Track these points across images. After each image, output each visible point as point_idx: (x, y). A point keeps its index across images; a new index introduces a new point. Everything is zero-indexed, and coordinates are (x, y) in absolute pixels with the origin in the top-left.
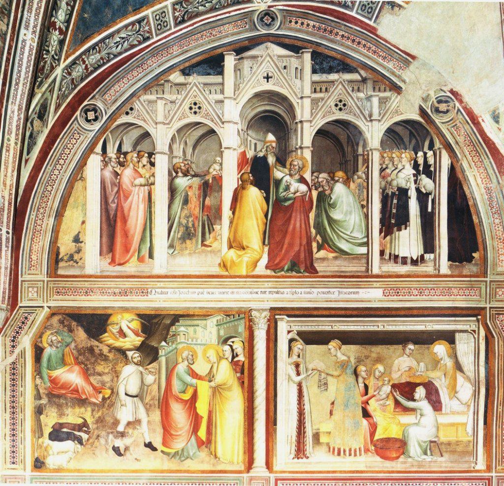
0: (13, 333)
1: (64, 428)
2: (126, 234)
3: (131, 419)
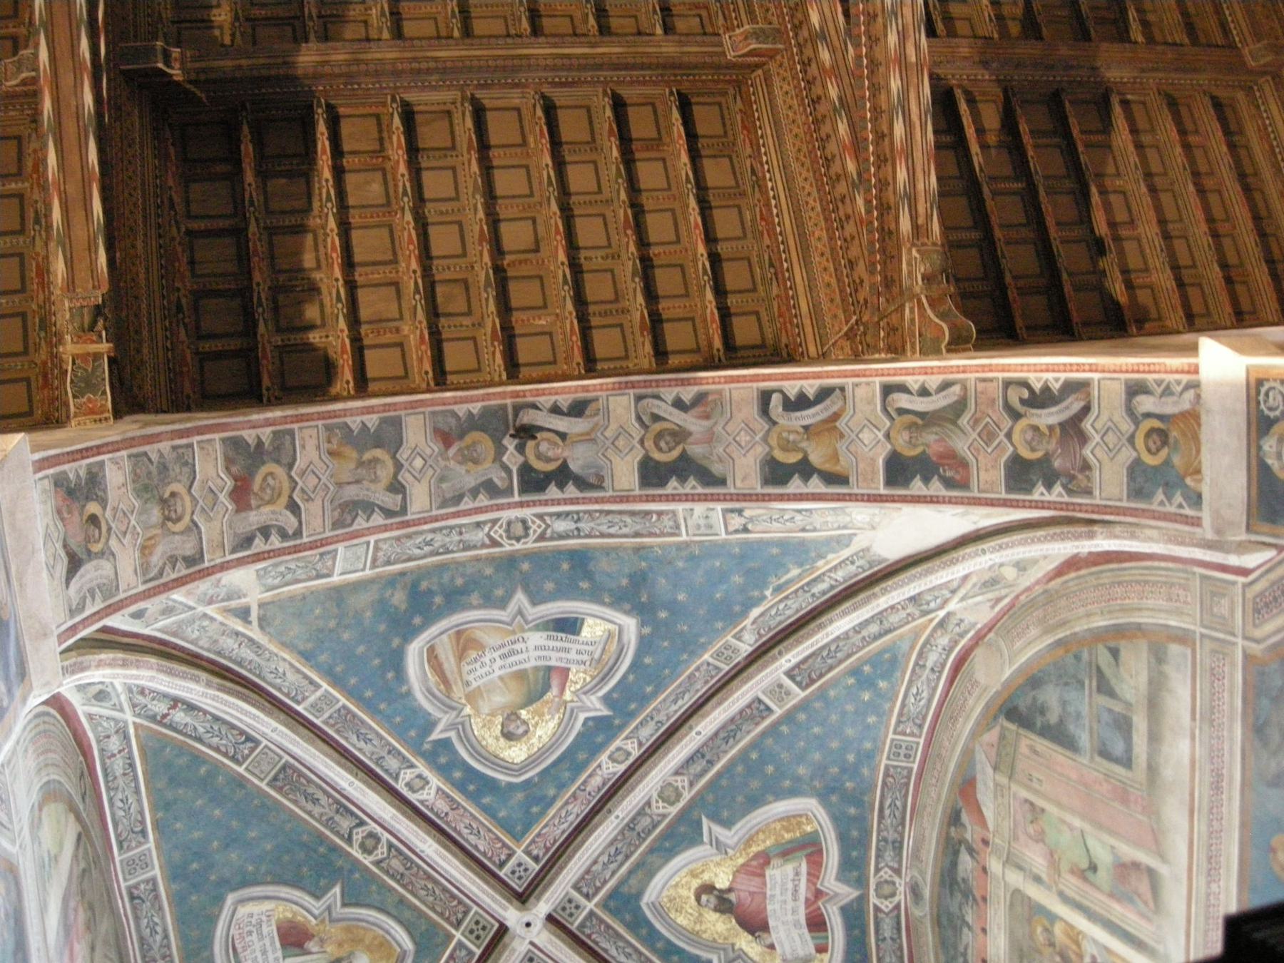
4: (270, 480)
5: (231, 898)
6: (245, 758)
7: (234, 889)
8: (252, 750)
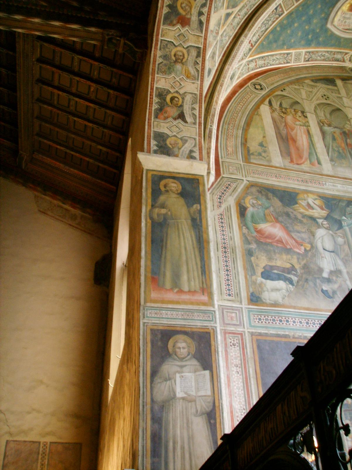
0: (219, 193)
1: (274, 270)
2: (298, 149)
3: (332, 269)
4: (183, 5)
5: (329, 26)
6: (283, 11)
7: (327, 23)
8: (281, 7)
